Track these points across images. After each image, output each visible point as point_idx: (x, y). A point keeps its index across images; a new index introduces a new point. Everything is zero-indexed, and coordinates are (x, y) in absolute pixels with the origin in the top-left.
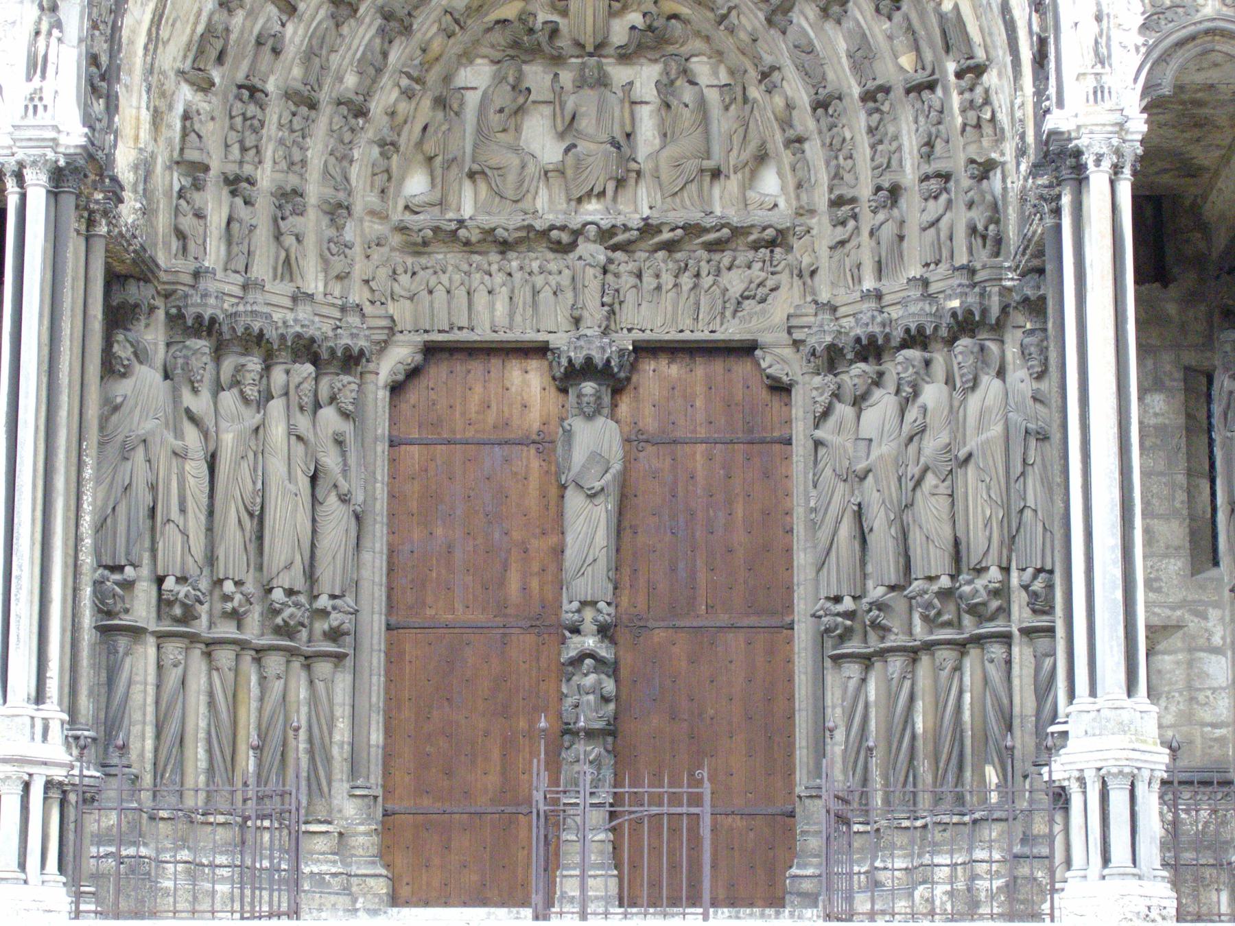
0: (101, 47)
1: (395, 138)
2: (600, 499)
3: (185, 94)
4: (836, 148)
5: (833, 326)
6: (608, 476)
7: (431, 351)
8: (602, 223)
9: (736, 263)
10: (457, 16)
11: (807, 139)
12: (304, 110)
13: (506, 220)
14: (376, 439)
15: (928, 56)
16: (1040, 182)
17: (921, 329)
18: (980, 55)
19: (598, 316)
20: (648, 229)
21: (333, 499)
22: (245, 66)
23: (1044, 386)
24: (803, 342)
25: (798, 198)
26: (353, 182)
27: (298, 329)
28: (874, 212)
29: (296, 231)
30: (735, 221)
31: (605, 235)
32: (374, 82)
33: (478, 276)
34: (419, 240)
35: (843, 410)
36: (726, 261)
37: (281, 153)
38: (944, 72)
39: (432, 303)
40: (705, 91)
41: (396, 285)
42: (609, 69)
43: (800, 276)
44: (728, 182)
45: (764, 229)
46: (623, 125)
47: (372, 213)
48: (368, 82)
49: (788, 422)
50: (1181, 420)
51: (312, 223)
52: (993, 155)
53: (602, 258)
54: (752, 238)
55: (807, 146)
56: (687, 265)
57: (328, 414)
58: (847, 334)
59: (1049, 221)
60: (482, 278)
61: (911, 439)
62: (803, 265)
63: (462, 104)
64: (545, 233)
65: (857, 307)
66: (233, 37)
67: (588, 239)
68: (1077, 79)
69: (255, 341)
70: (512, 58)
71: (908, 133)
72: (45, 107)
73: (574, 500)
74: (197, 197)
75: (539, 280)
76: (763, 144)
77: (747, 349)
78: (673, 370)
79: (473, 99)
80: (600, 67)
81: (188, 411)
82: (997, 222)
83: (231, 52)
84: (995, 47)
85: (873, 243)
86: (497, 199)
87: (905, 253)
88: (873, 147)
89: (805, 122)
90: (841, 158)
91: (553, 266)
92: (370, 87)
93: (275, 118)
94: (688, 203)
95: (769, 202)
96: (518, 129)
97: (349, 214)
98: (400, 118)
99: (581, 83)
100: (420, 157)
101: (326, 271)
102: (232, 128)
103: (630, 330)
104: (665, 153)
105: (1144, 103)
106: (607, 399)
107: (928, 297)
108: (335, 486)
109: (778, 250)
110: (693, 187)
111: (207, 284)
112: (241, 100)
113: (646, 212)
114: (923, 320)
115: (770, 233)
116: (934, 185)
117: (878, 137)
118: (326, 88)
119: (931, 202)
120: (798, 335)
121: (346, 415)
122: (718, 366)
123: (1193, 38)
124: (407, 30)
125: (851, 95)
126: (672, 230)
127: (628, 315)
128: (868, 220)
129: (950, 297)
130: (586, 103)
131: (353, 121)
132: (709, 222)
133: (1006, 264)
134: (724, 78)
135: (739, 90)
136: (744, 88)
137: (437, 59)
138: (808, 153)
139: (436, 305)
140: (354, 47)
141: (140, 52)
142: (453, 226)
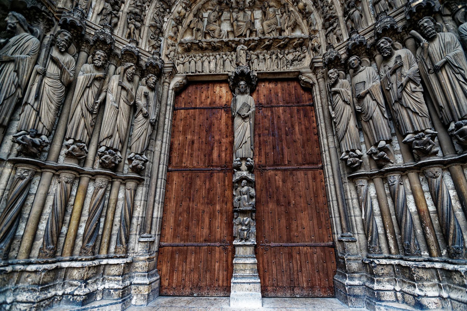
2: (248, 119)
6: (250, 112)
20: (261, 40)
21: (140, 116)
24: (318, 68)
30: (289, 37)
31: (247, 43)
34: (186, 46)
36: (286, 52)
44: (285, 33)
47: (172, 37)
55: (312, 16)
64: (227, 43)
73: (238, 121)
79: (206, 19)
108: (141, 111)
110: (273, 33)
120: (316, 65)
121: (152, 89)
122: (285, 84)
142: (197, 42)
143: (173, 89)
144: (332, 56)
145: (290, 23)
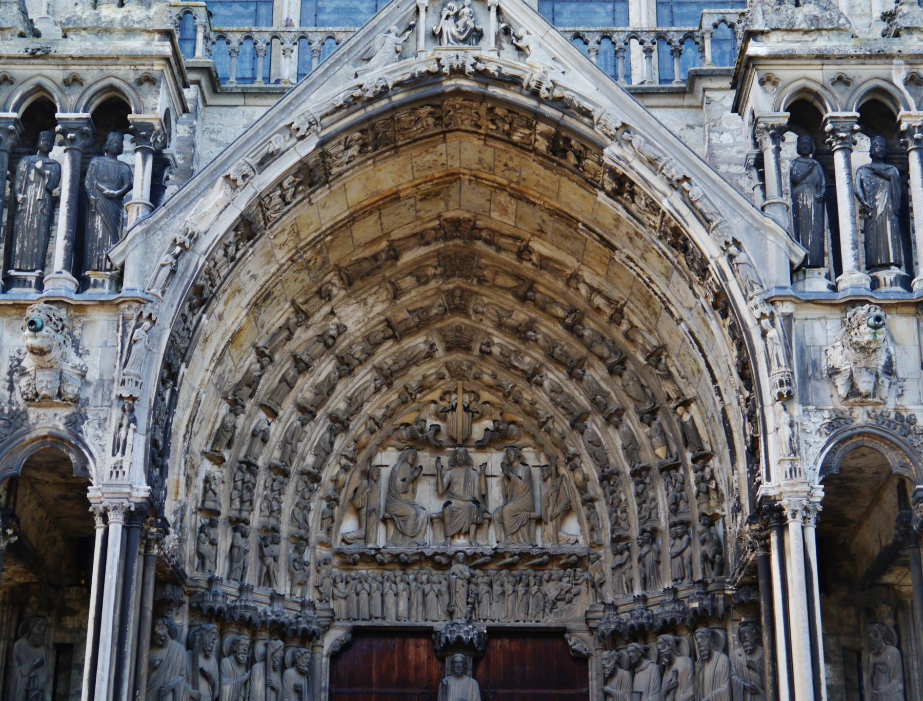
0: (159, 436)
1: (337, 496)
3: (207, 466)
4: (615, 505)
5: (614, 619)
7: (357, 632)
8: (468, 551)
9: (553, 577)
10: (377, 420)
11: (597, 500)
12: (281, 478)
13: (405, 548)
14: (321, 690)
15: (674, 449)
16: (753, 527)
17: (673, 620)
18: (708, 448)
19: (464, 611)
20: (497, 555)
22: (244, 449)
23: (755, 658)
24: (596, 629)
25: (591, 537)
26: (310, 525)
27: (274, 617)
28: (641, 546)
29: (274, 554)
30: (551, 552)
31: (470, 559)
32: (325, 461)
33: (388, 584)
34: (351, 561)
35: (623, 673)
36: (546, 577)
37: (265, 504)
38: (684, 458)
39: (358, 602)
40: (532, 469)
41: (335, 590)
42: (471, 455)
43: (593, 586)
45: (570, 556)
46: (480, 490)
48: (322, 460)
49: (585, 681)
50: (842, 682)
51: (284, 549)
52: (717, 511)
53: (467, 574)
54: (562, 562)
55: (596, 504)
56: (521, 579)
57: (291, 672)
58: (625, 624)
59: (760, 553)
60: (391, 586)
61: (668, 692)
62: (596, 579)
63: (379, 476)
64: (431, 558)
65: (630, 607)
66: (238, 431)
67: (458, 562)
68: (779, 463)
69: (249, 625)
70: (411, 448)
71: (662, 497)
72: (124, 473)
74: (212, 532)
75: (427, 587)
76: (569, 502)
77: (560, 633)
78: (513, 645)
79: (385, 473)
80: (466, 453)
81: (202, 670)
82: (721, 553)
83: (236, 440)
84: (717, 444)
85: (641, 566)
86: (401, 536)
87: (661, 573)
88: (639, 505)
89: (595, 489)
90: (619, 512)
91: (435, 579)
92: (322, 464)
93: (262, 482)
94: (522, 540)
95: (573, 539)
96: (414, 492)
97: (307, 544)
98: (340, 484)
99: (454, 463)
100: (352, 509)
101: (292, 580)
102: (235, 488)
103: (485, 620)
104: (507, 508)
105: (821, 478)
106: (470, 665)
107: (677, 601)
109: (578, 569)
110: (524, 529)
111: (221, 589)
112: (241, 471)
113: (495, 545)
114: (674, 615)
115: (574, 558)
116: (679, 529)
117: (643, 499)
118: (294, 464)
119: (678, 541)
120: (592, 624)
121: (301, 673)
123: (850, 437)
124: (345, 428)
125: (624, 473)
126: (512, 556)
127: (485, 610)
128: (636, 552)
129: (692, 601)
130: (458, 474)
131: (311, 485)
132: (535, 551)
133: (728, 580)
134: (543, 461)
135: (553, 468)
136: (557, 468)
137: (364, 447)
138: (597, 509)
139: (362, 602)
140: (312, 439)
141: (181, 439)
142: (373, 552)
143: (327, 656)
144: (608, 630)
145: (558, 510)
